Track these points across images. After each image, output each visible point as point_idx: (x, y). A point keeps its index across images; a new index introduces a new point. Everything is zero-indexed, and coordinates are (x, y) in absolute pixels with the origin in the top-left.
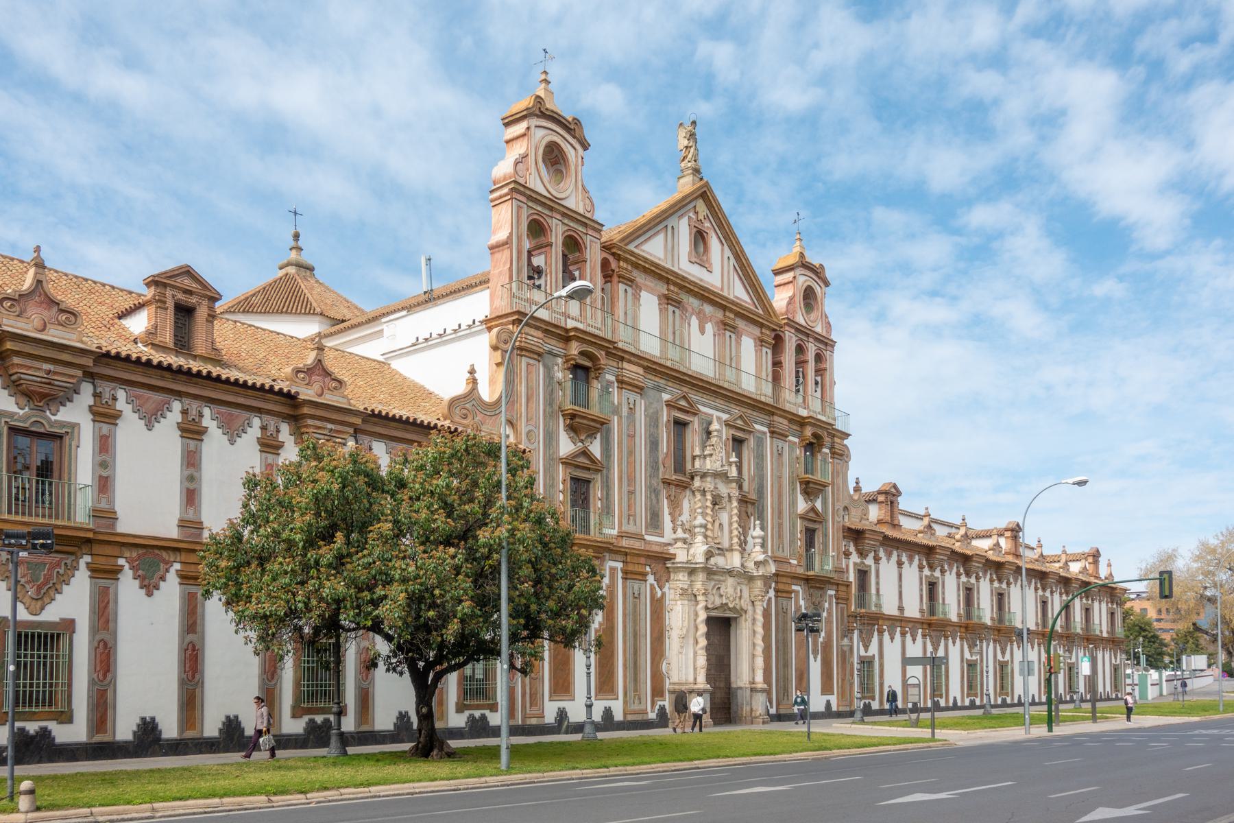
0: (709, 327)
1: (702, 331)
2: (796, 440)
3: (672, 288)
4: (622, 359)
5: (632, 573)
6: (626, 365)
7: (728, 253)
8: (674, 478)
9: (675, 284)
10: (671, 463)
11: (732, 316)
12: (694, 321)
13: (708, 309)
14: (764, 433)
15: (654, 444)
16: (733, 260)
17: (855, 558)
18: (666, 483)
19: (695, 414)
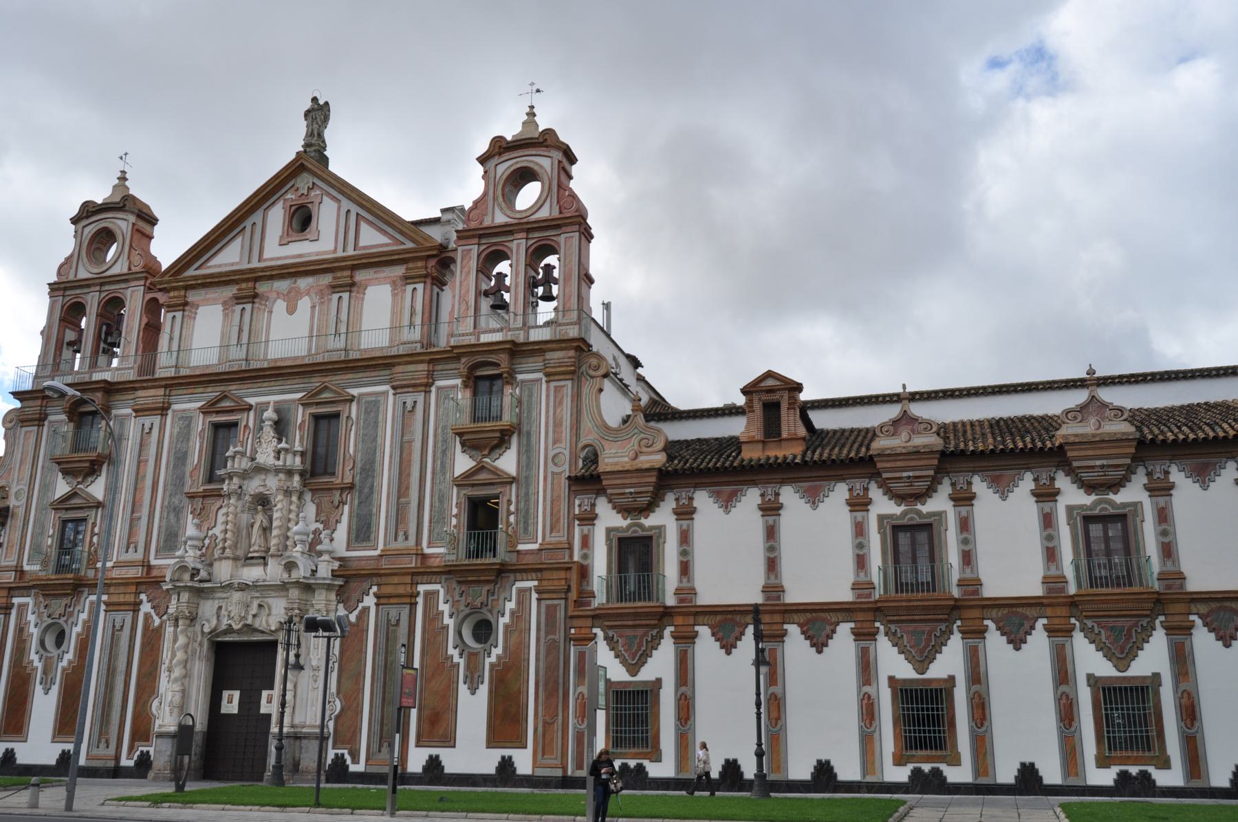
0: (304, 304)
1: (291, 310)
2: (458, 382)
3: (244, 285)
4: (135, 389)
5: (390, 597)
6: (140, 393)
7: (346, 204)
8: (201, 489)
9: (247, 280)
10: (201, 474)
11: (347, 273)
12: (280, 306)
13: (303, 283)
14: (385, 393)
15: (180, 458)
16: (355, 209)
17: (609, 518)
18: (192, 496)
19: (249, 408)
